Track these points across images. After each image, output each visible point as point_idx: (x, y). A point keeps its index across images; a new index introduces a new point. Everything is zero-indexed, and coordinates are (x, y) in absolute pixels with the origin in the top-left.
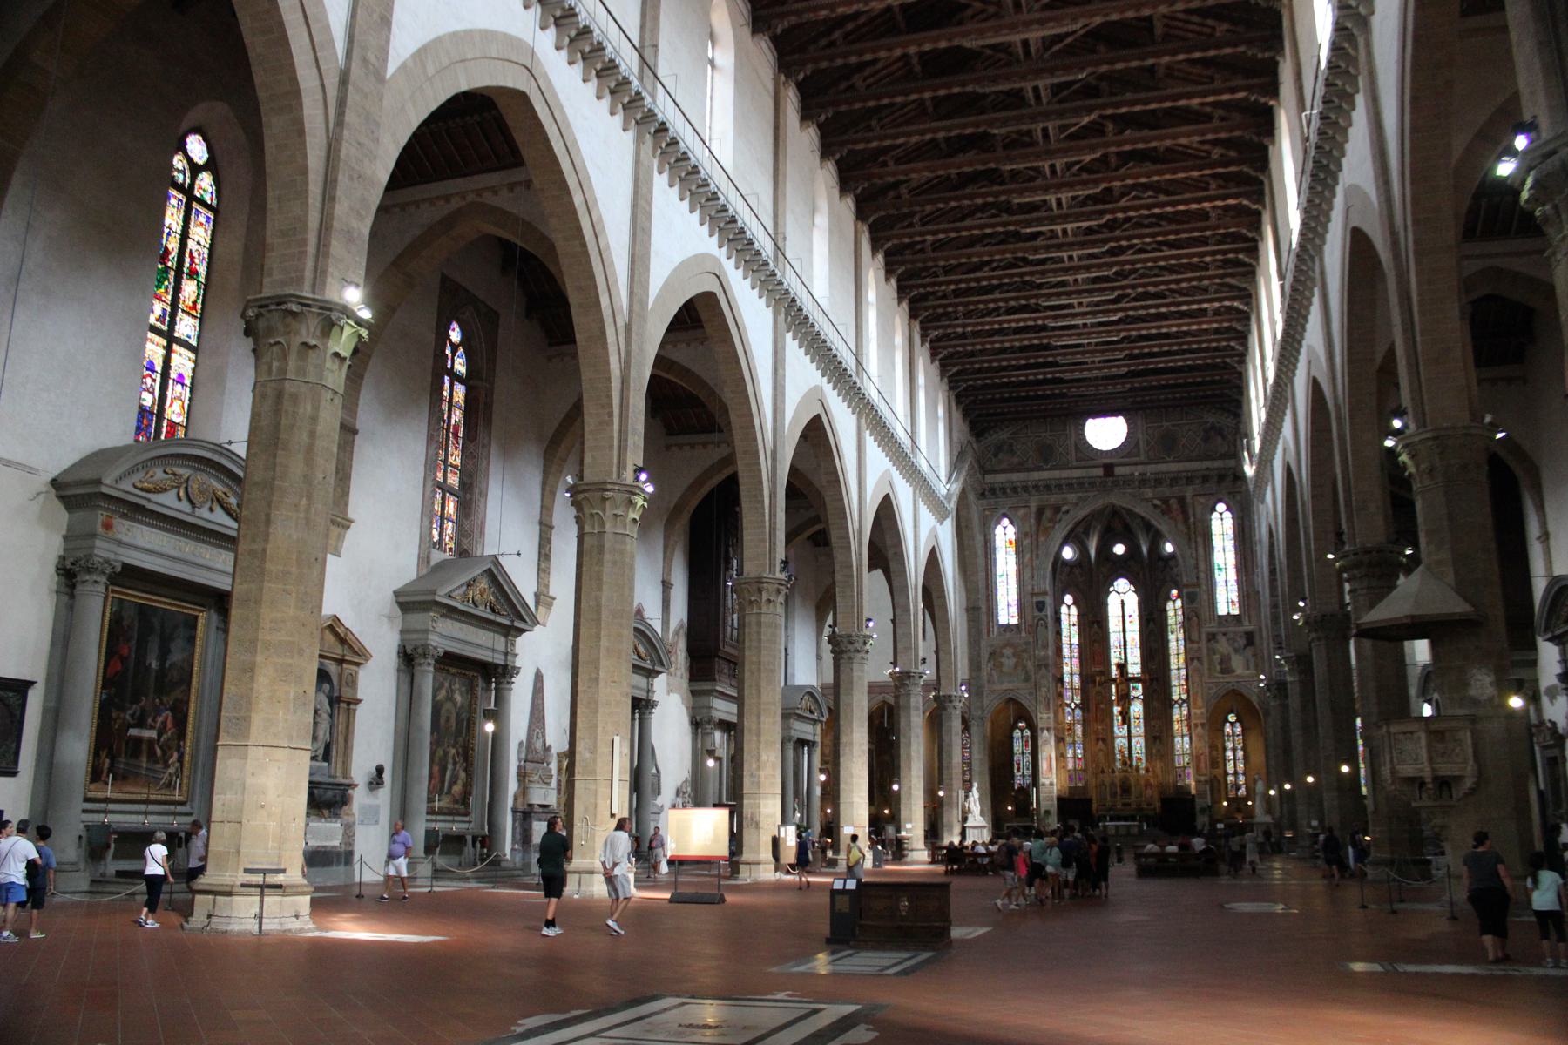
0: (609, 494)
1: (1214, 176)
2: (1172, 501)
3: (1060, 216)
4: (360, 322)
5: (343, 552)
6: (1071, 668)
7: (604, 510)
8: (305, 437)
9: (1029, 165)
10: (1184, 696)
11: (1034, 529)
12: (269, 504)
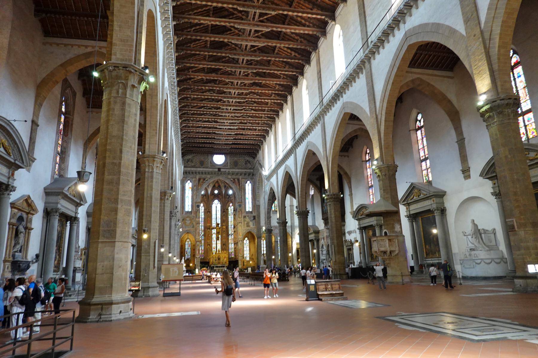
0: (156, 159)
1: (275, 94)
2: (236, 180)
3: (234, 97)
4: (148, 83)
5: (31, 171)
6: (202, 224)
7: (154, 165)
8: (133, 121)
9: (229, 81)
10: (232, 233)
11: (197, 184)
12: (121, 145)
